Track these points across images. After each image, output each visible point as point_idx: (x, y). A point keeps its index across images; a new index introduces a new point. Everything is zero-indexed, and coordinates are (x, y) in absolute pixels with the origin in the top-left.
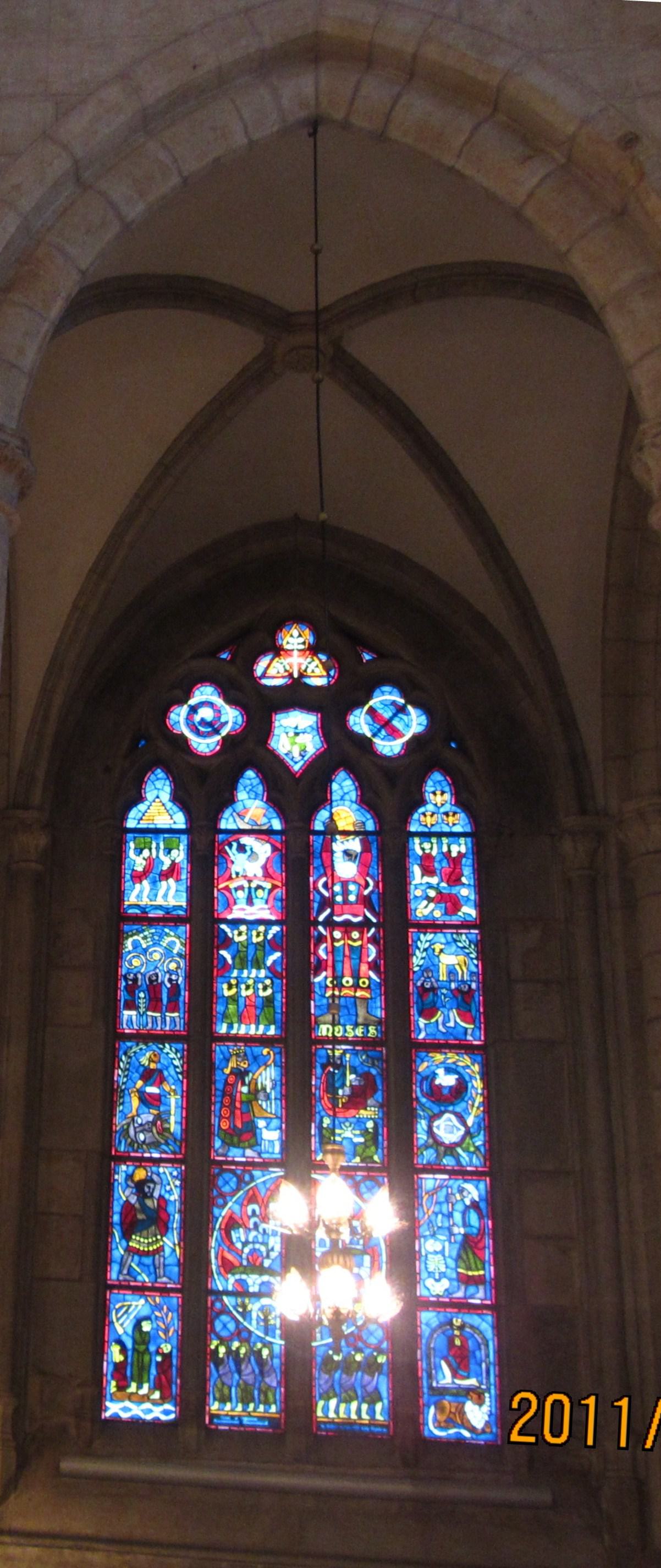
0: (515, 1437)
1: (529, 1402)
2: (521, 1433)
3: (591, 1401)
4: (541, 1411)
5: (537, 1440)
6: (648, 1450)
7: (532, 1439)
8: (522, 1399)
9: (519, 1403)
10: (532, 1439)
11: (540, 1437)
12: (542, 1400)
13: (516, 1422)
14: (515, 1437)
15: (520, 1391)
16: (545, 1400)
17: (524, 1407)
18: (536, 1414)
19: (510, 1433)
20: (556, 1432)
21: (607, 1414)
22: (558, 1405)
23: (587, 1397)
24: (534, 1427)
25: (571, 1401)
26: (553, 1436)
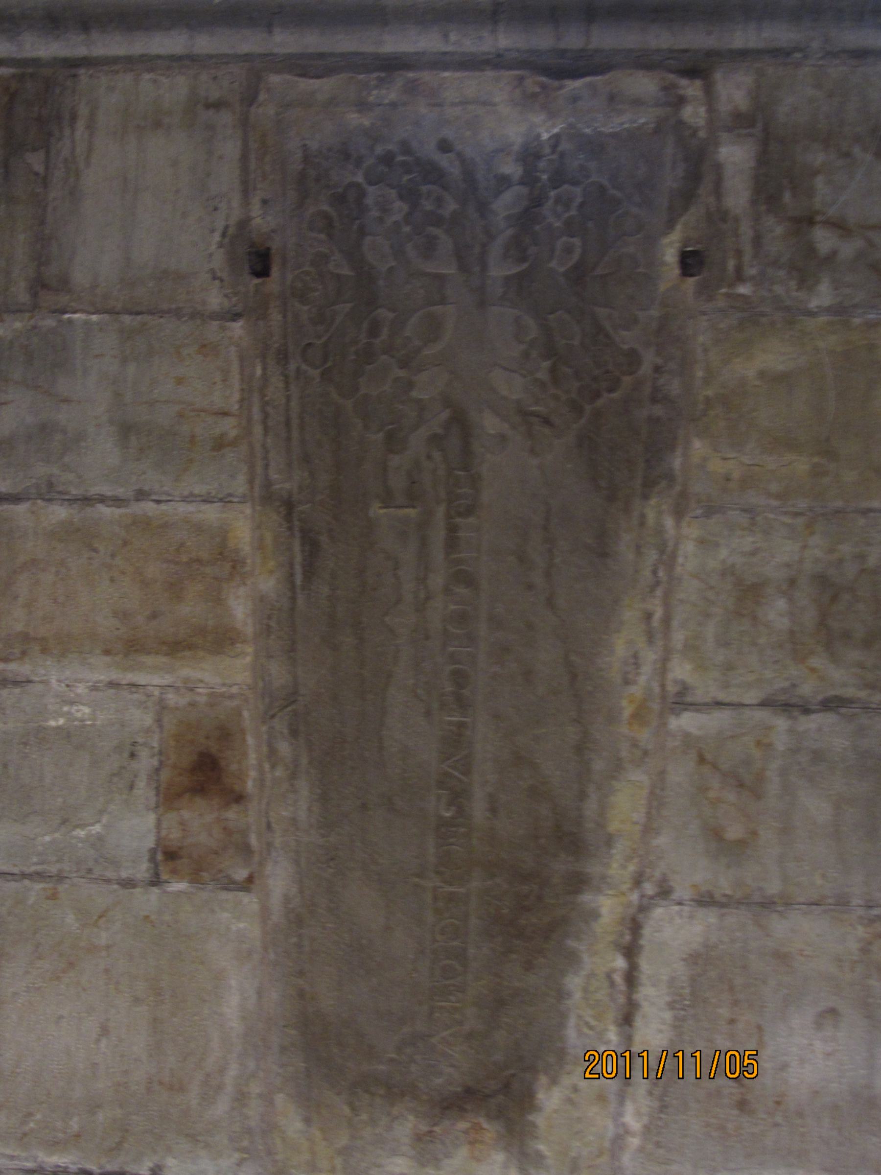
0: (587, 1075)
1: (595, 1056)
2: (590, 1073)
4: (600, 1062)
6: (659, 1078)
7: (597, 1076)
9: (589, 1057)
10: (597, 1076)
11: (601, 1075)
12: (601, 1056)
14: (587, 1075)
17: (592, 1058)
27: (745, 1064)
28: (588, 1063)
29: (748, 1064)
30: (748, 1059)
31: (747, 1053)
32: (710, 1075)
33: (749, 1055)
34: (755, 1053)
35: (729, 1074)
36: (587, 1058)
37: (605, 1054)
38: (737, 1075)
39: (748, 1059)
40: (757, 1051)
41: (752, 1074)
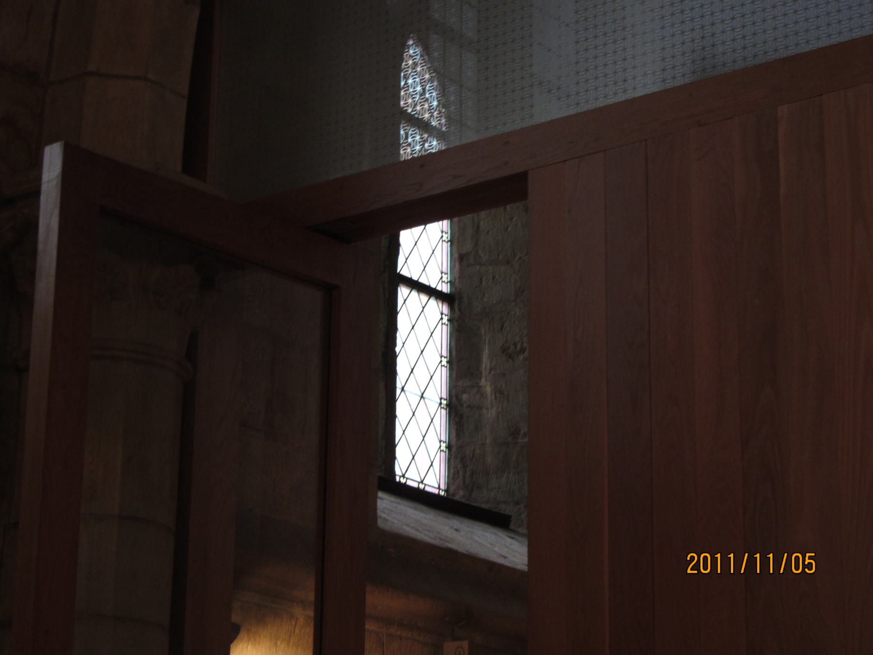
0: (689, 571)
2: (691, 570)
3: (719, 556)
5: (698, 572)
7: (696, 572)
8: (691, 556)
9: (690, 558)
10: (696, 572)
13: (689, 565)
14: (689, 571)
15: (690, 553)
16: (700, 556)
18: (697, 562)
19: (687, 570)
20: (705, 568)
21: (725, 562)
22: (705, 558)
23: (717, 554)
24: (696, 567)
25: (711, 556)
26: (704, 570)
27: (806, 563)
28: (690, 562)
29: (808, 563)
30: (809, 559)
31: (808, 555)
32: (780, 571)
33: (809, 556)
34: (813, 554)
35: (794, 571)
36: (688, 559)
37: (702, 556)
38: (800, 571)
39: (809, 559)
40: (815, 553)
41: (811, 570)
